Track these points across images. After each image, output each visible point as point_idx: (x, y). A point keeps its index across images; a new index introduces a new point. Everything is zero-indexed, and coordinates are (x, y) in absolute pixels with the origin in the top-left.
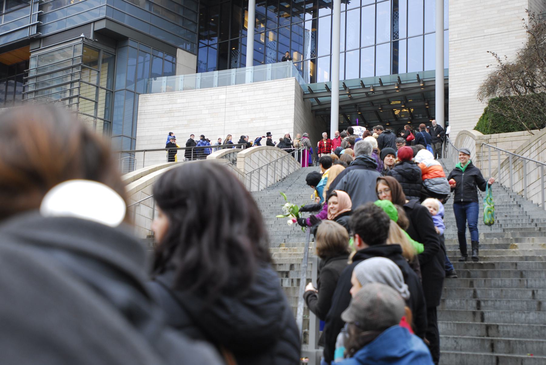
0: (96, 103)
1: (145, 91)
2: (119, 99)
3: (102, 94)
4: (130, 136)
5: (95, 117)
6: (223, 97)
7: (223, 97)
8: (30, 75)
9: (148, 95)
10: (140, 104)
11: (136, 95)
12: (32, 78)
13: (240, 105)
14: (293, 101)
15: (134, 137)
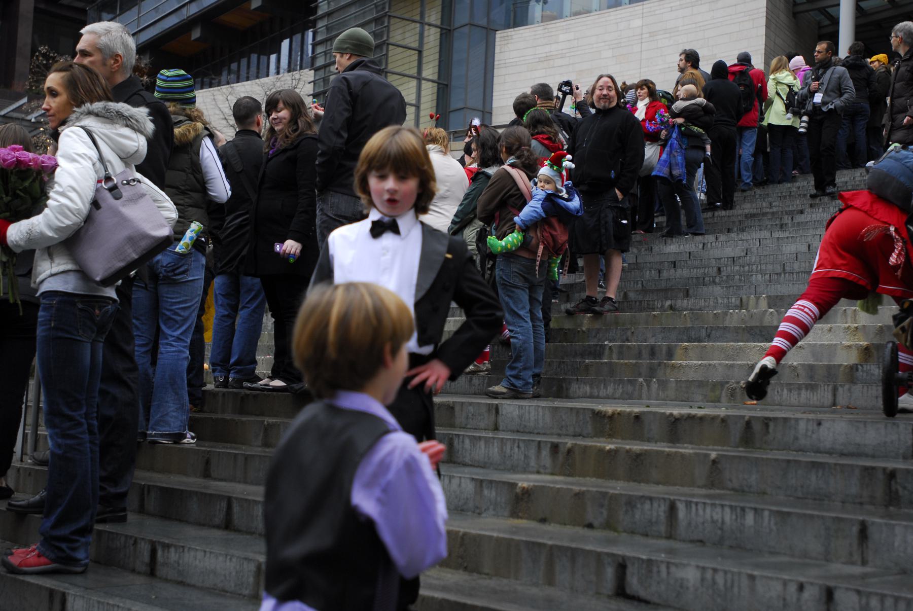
0: (420, 52)
1: (512, 22)
2: (459, 44)
3: (432, 37)
4: (480, 108)
5: (419, 78)
6: (637, 23)
7: (637, 23)
8: (320, 12)
9: (510, 32)
10: (497, 50)
11: (489, 33)
12: (322, 17)
13: (667, 35)
14: (763, 21)
15: (487, 110)
